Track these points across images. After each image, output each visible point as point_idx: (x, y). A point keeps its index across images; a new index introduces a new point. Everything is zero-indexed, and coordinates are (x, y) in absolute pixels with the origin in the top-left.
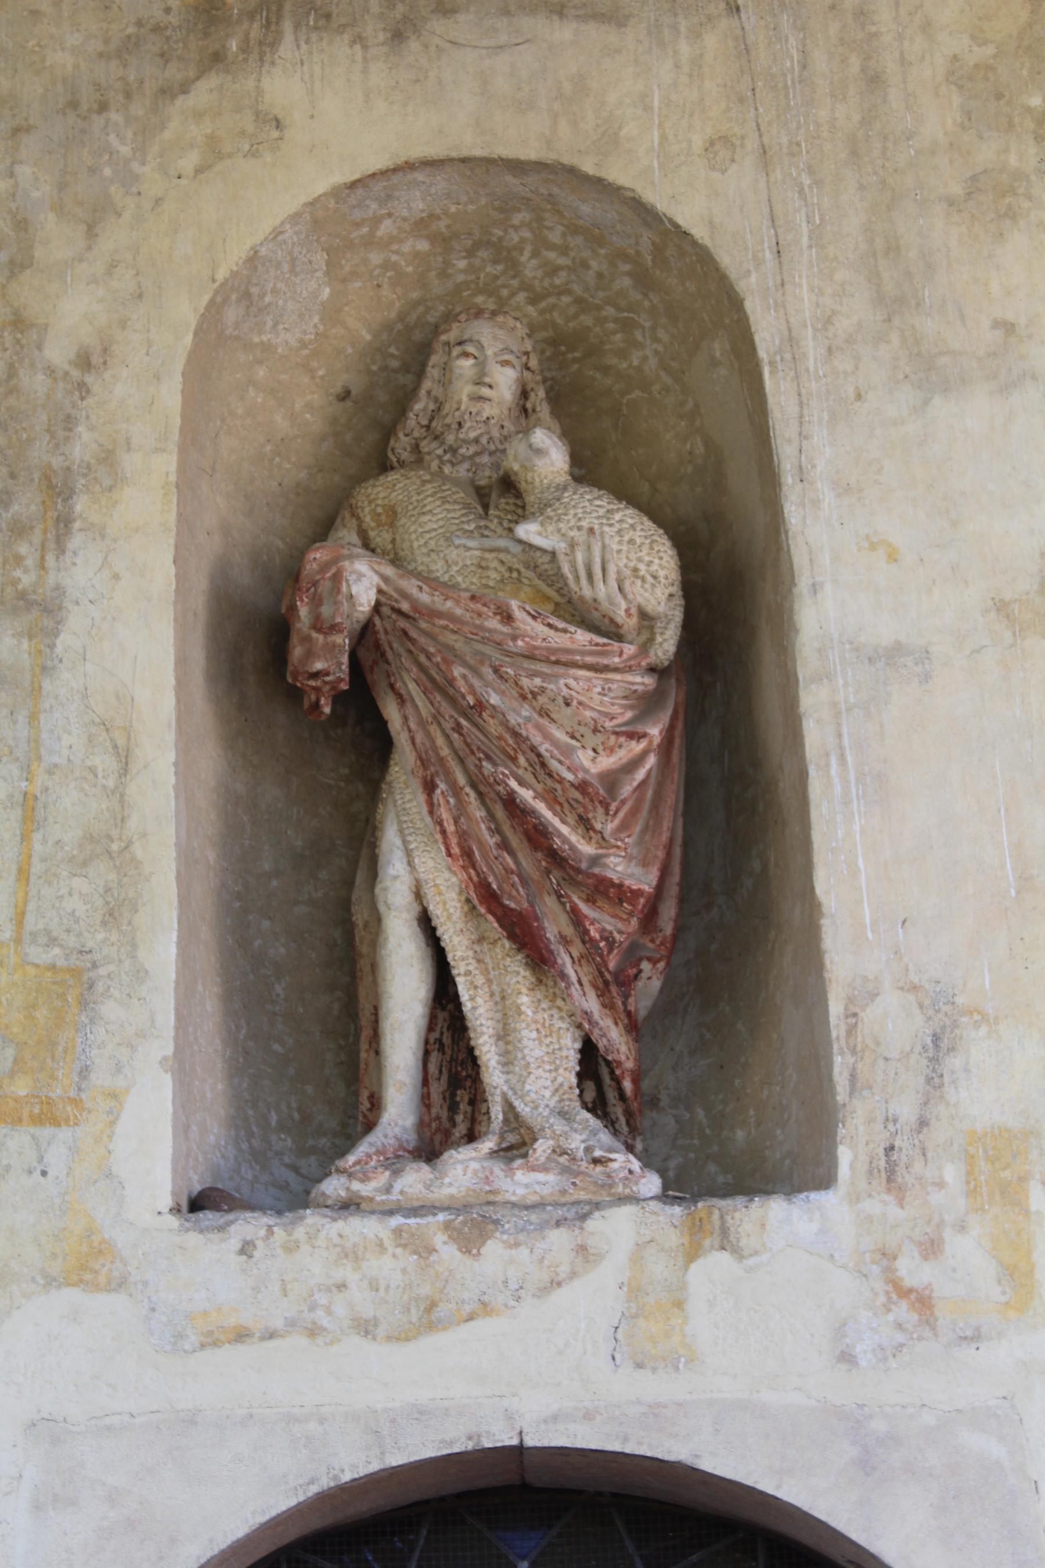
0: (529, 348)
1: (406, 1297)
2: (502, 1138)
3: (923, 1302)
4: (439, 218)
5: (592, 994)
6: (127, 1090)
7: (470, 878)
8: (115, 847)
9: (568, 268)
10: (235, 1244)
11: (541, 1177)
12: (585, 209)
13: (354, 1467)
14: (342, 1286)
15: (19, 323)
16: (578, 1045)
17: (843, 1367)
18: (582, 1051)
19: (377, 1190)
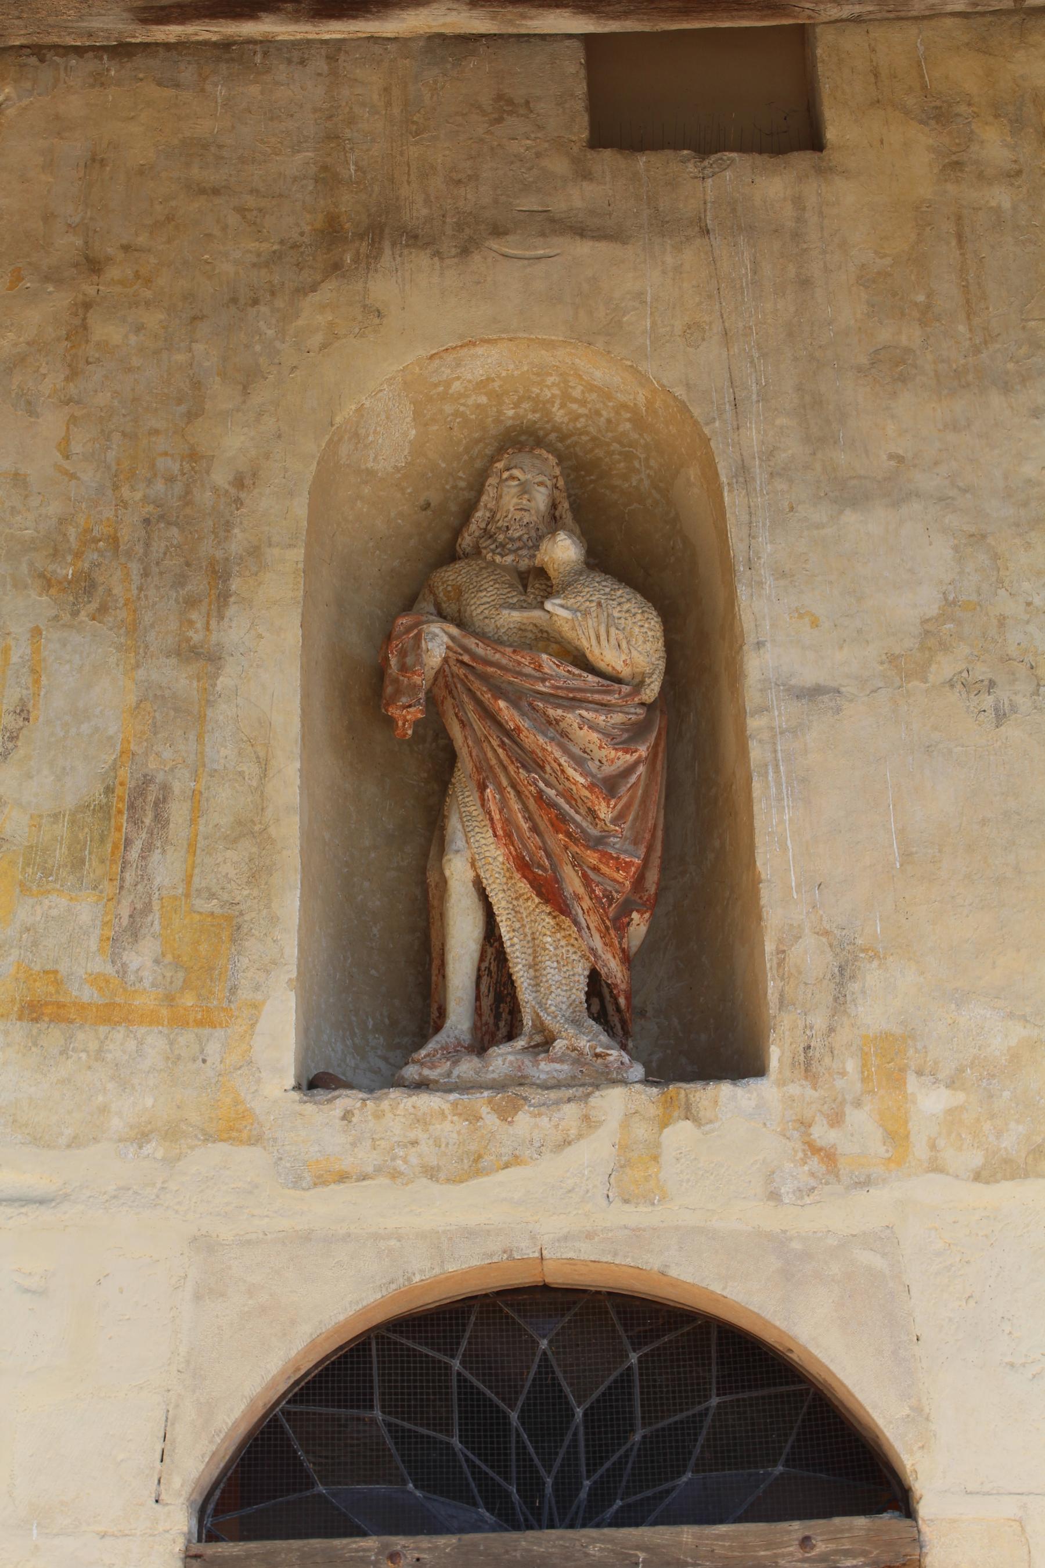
0: (558, 473)
1: (460, 1151)
2: (531, 1038)
3: (829, 1156)
4: (493, 380)
5: (597, 936)
6: (264, 1002)
7: (510, 853)
8: (257, 828)
9: (586, 415)
10: (339, 1112)
11: (558, 1066)
12: (598, 374)
13: (422, 1271)
14: (414, 1143)
15: (193, 456)
16: (587, 973)
17: (772, 1203)
18: (590, 977)
19: (440, 1075)
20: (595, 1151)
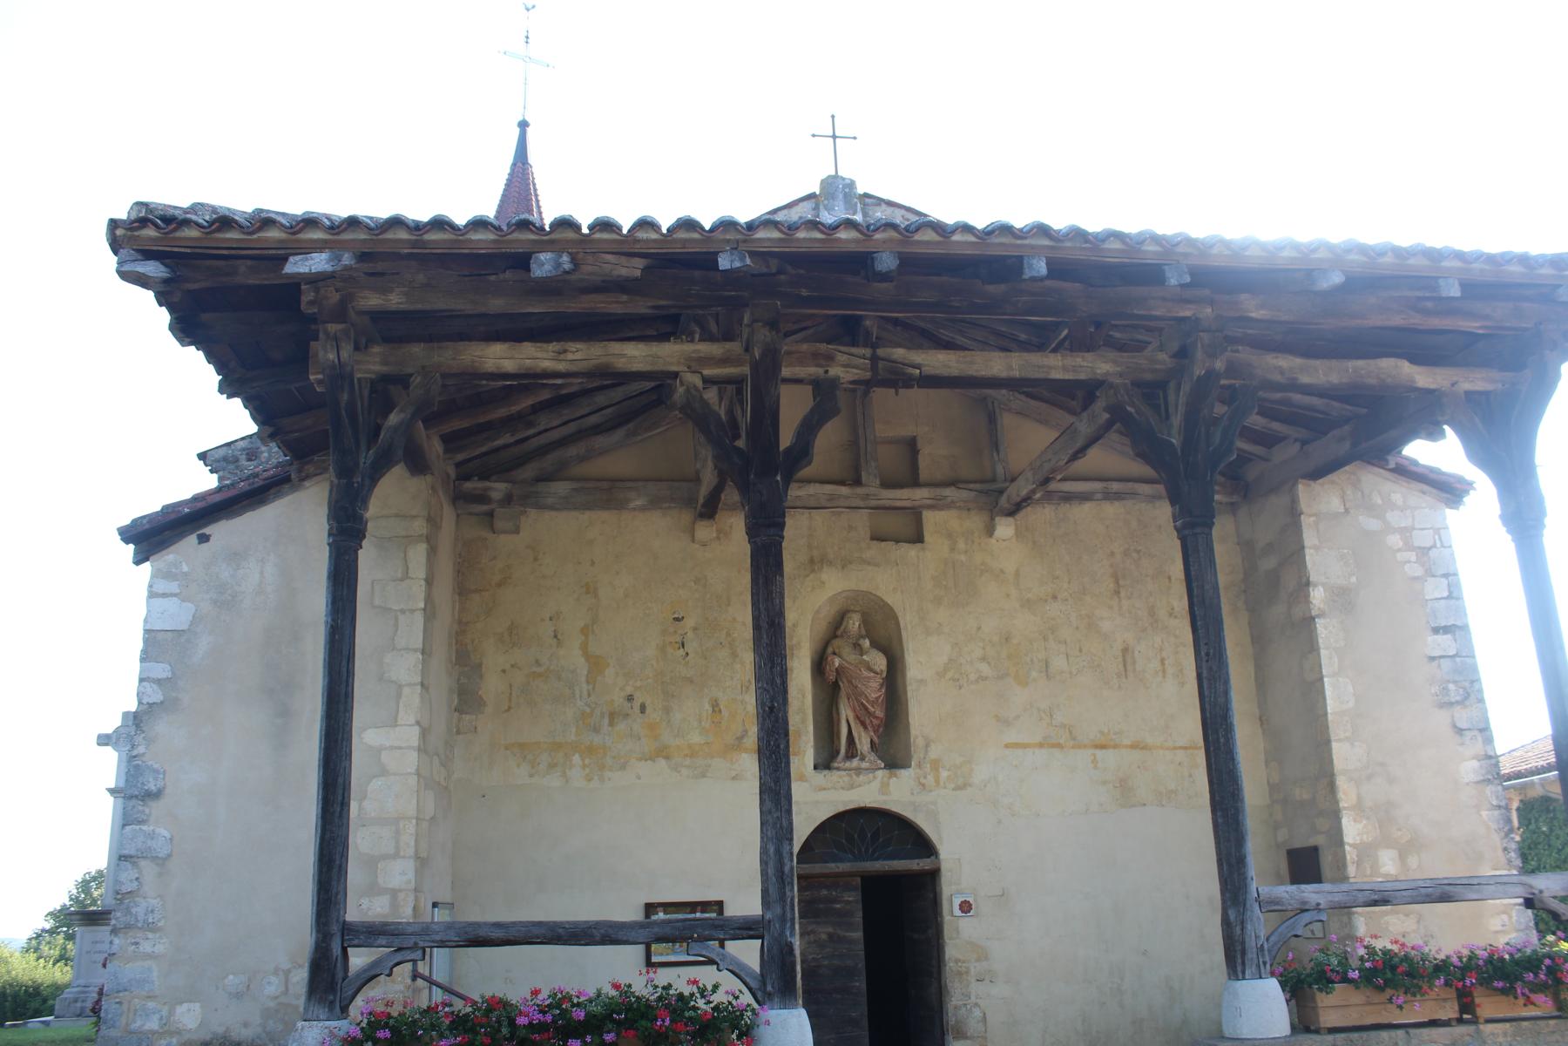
20: (876, 785)
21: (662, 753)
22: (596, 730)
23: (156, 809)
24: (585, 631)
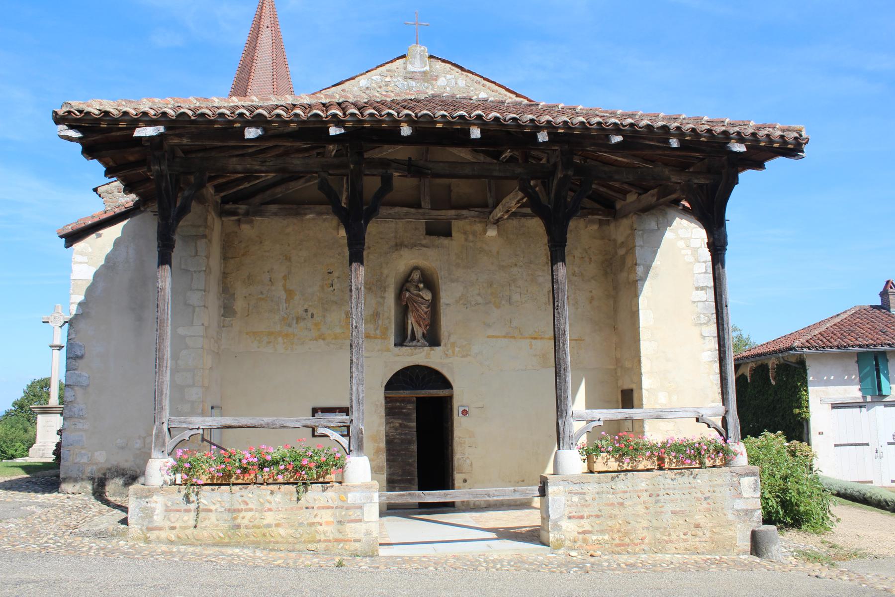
20: (424, 354)
21: (322, 337)
22: (290, 326)
23: (80, 363)
24: (285, 278)
